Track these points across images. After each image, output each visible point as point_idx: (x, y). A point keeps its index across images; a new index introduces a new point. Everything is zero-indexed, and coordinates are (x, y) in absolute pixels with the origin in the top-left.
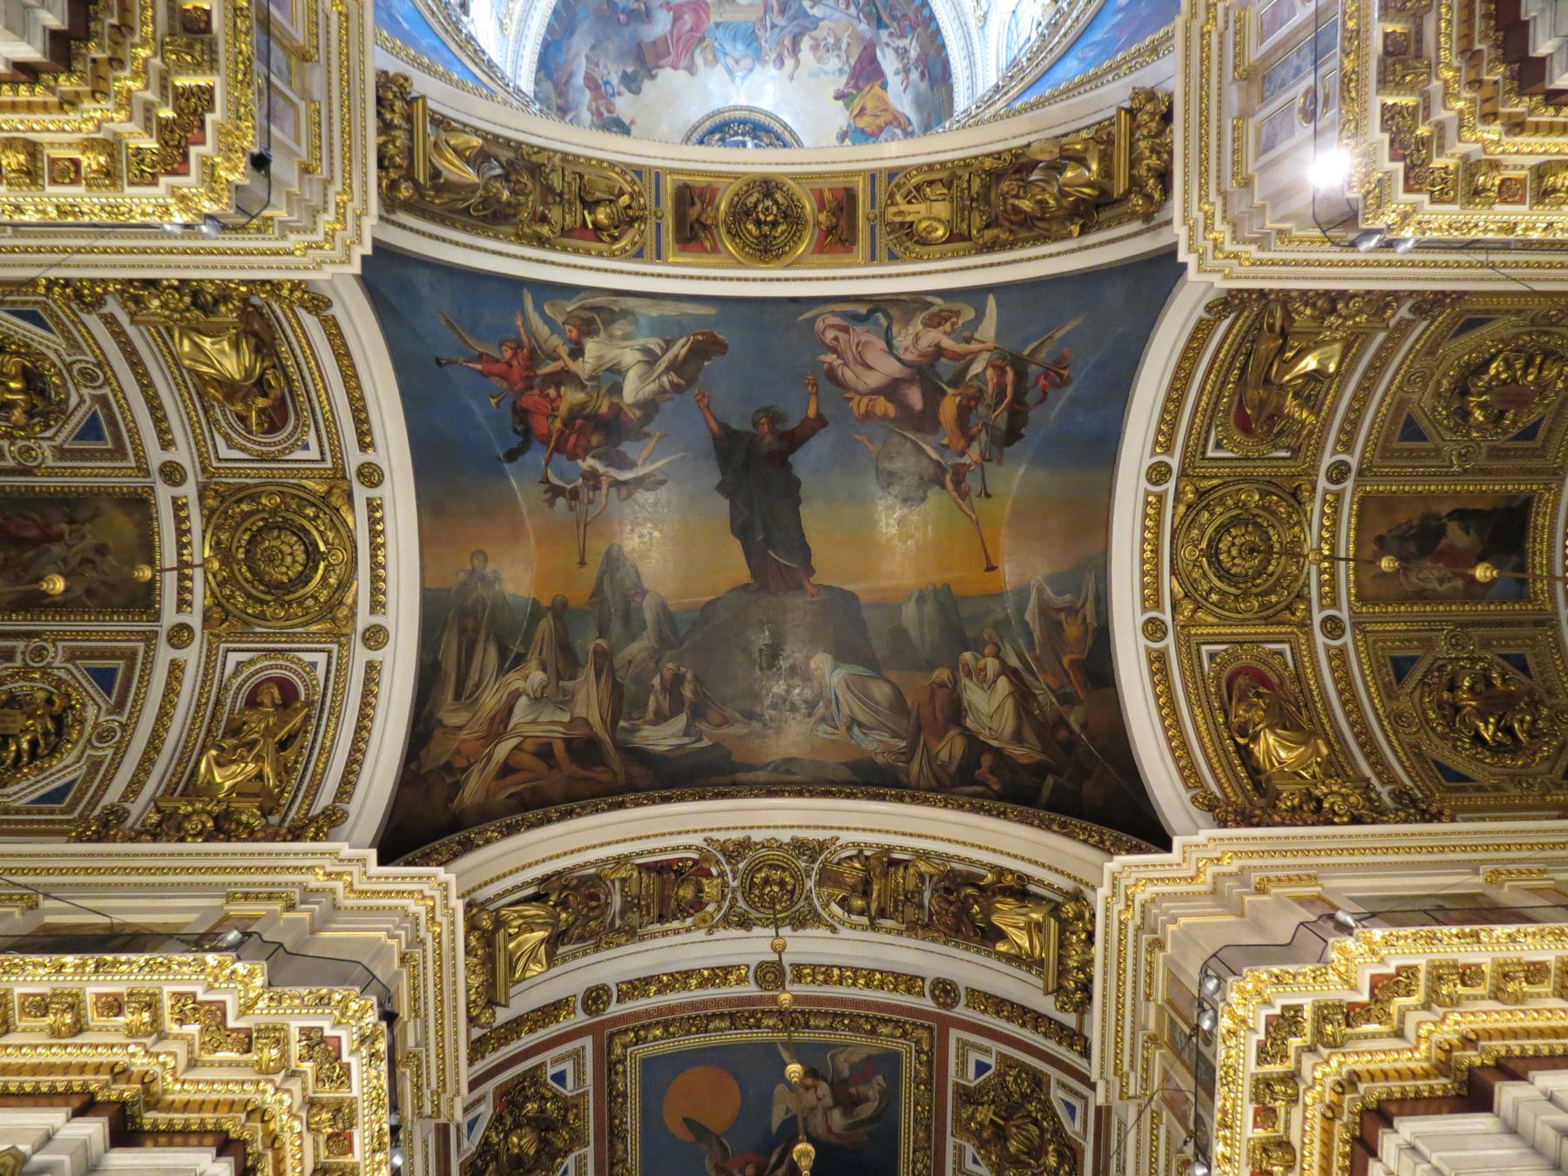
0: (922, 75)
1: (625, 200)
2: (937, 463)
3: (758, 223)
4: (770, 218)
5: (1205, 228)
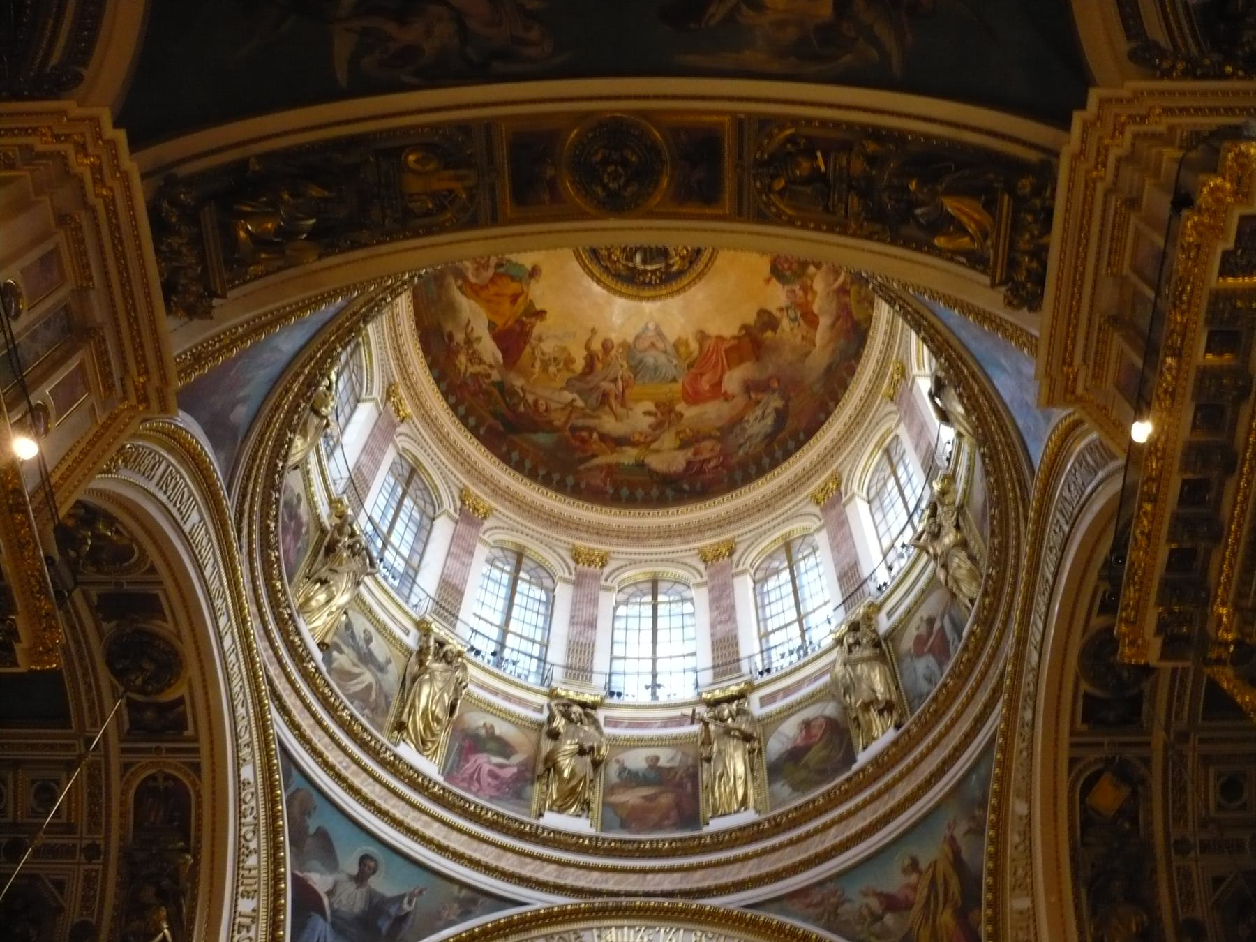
0: (451, 337)
1: (779, 184)
3: (624, 163)
4: (611, 168)
5: (100, 170)
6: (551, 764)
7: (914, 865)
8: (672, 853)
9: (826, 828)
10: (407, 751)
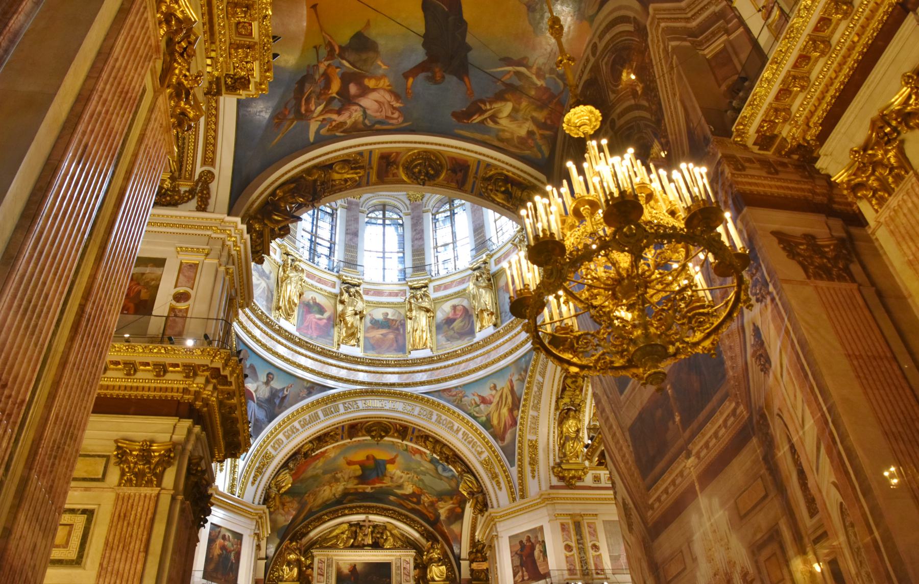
1: (490, 187)
2: (343, 58)
6: (342, 317)
7: (495, 387)
8: (395, 366)
9: (460, 363)
10: (284, 324)
